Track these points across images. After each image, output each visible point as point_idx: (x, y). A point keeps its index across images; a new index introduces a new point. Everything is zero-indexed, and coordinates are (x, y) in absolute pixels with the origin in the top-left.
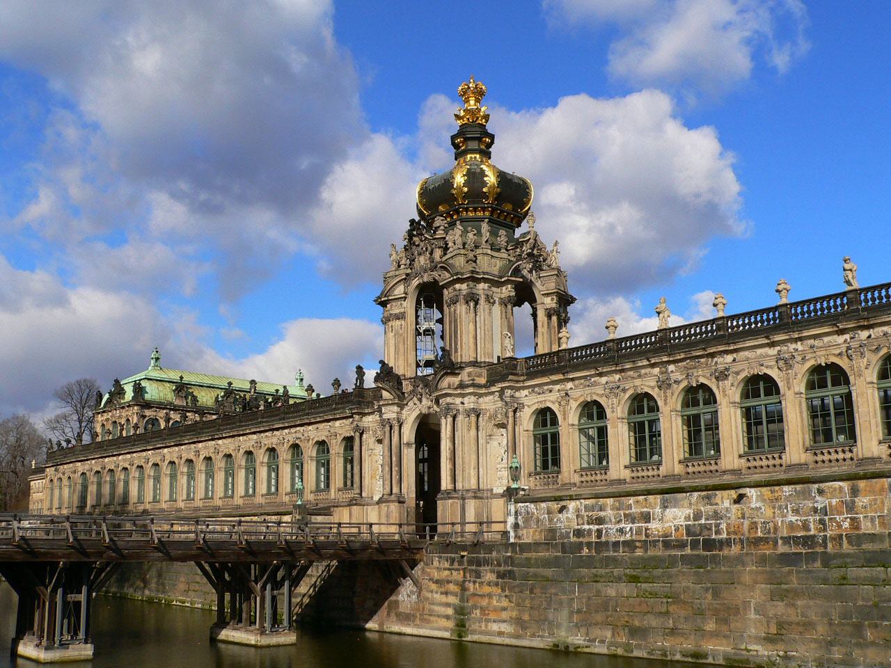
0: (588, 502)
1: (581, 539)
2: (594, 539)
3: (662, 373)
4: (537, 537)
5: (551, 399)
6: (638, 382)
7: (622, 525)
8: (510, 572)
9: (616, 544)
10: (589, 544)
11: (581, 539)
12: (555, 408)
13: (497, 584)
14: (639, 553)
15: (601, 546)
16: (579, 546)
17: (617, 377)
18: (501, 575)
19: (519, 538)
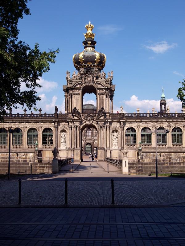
0: (166, 153)
1: (164, 162)
2: (168, 162)
3: (169, 123)
4: (150, 161)
5: (134, 125)
6: (161, 125)
7: (176, 159)
8: (141, 170)
9: (175, 163)
10: (167, 163)
11: (164, 162)
12: (135, 128)
13: (137, 173)
14: (182, 165)
15: (170, 164)
16: (164, 163)
17: (156, 123)
18: (137, 171)
19: (143, 161)
